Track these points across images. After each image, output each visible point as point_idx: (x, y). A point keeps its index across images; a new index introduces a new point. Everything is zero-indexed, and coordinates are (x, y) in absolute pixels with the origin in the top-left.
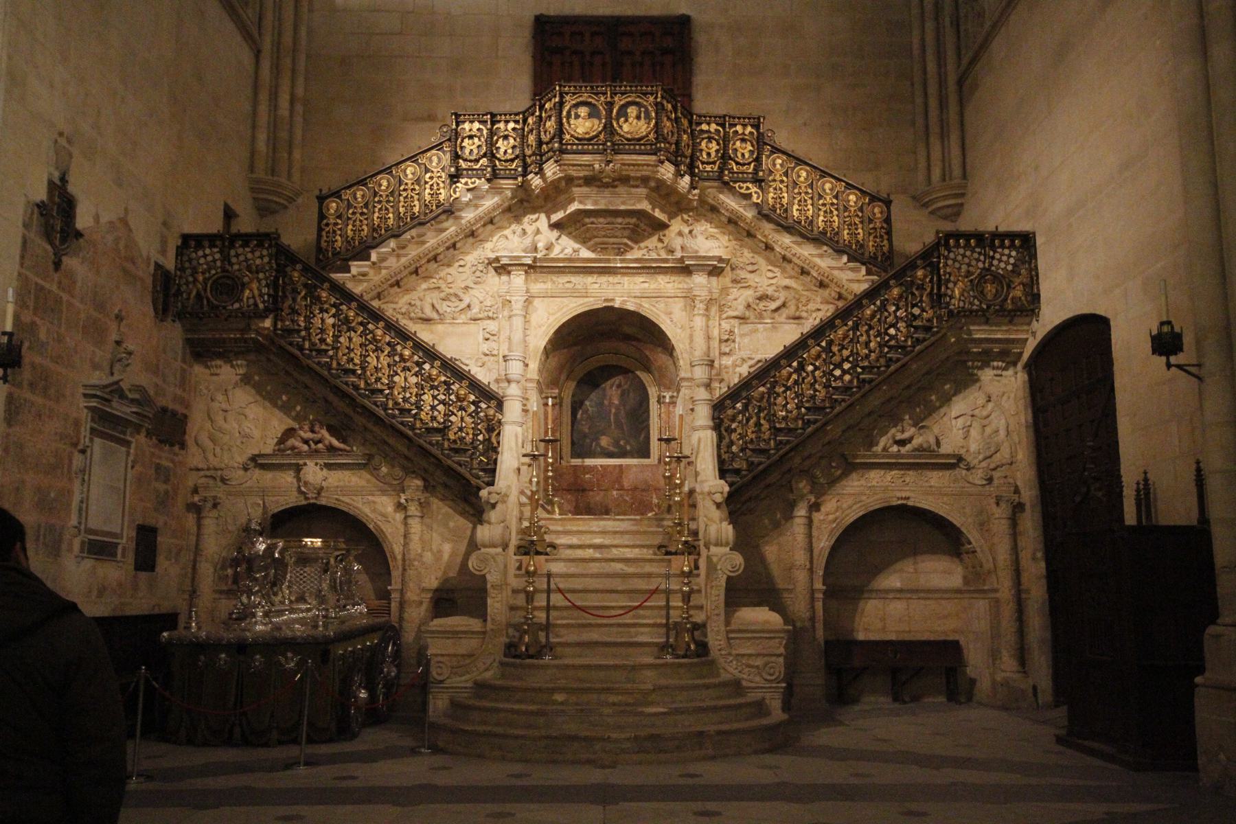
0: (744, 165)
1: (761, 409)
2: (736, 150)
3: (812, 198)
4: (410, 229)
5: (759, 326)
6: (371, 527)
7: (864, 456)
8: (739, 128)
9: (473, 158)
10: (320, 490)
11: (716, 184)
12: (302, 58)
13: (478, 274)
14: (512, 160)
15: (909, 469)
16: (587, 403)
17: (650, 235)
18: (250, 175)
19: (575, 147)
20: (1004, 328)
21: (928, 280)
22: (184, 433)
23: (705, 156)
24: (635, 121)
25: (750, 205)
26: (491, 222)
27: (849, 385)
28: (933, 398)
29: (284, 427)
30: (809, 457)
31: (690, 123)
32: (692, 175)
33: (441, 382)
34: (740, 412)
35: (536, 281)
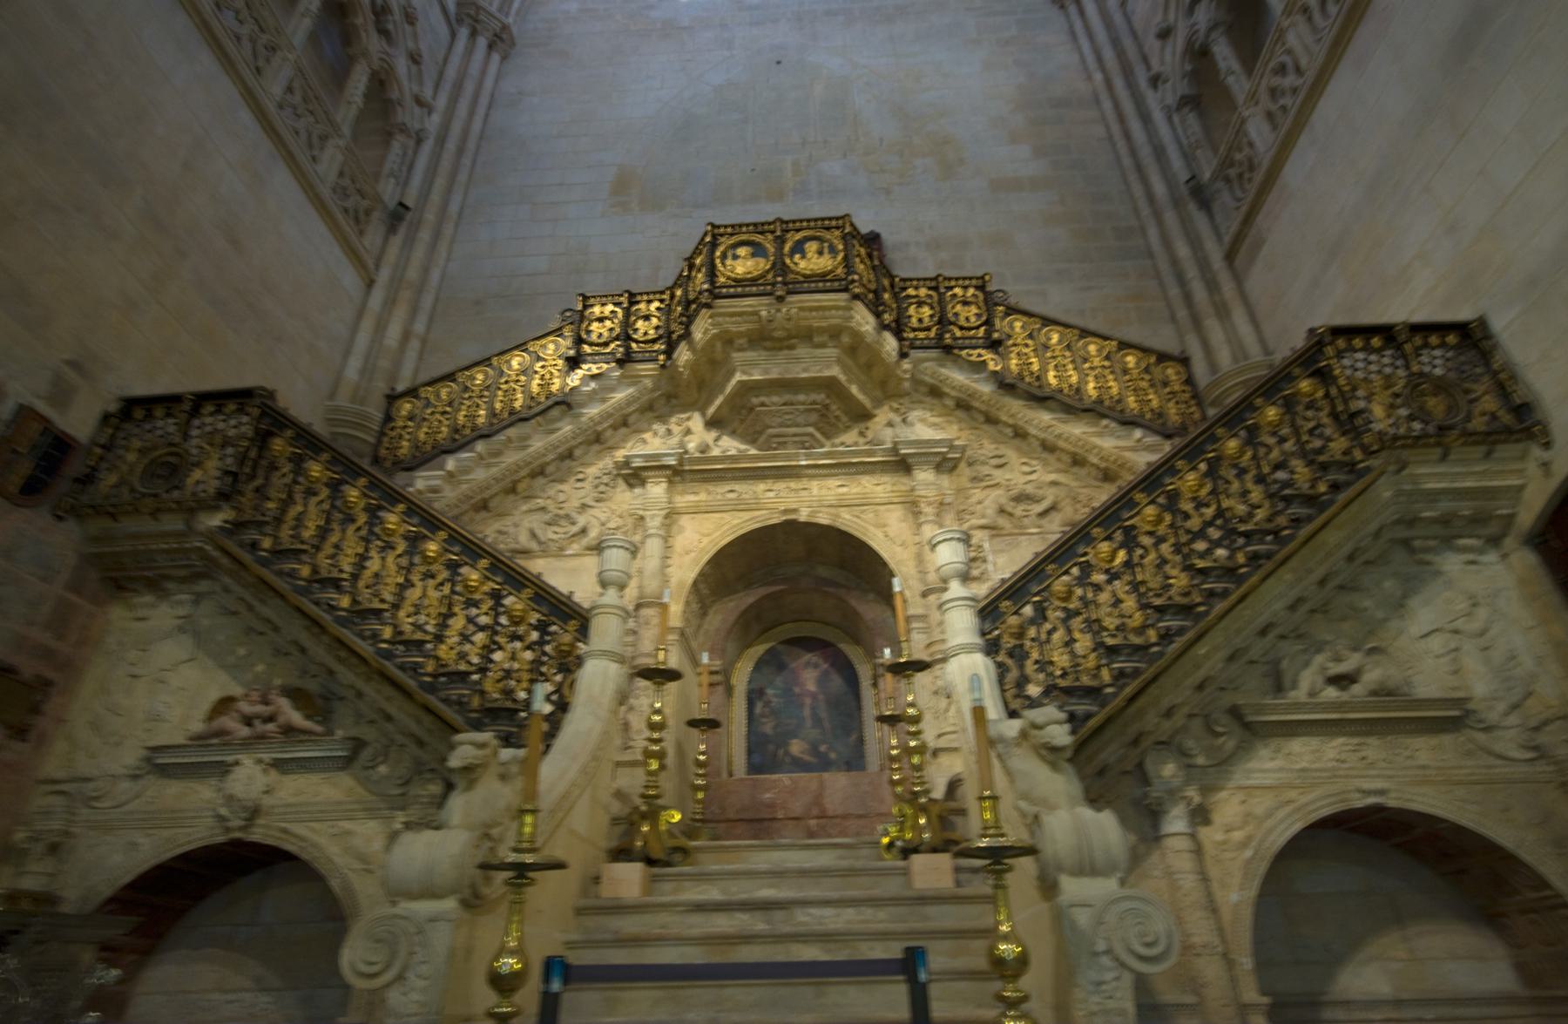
0: (970, 329)
1: (1071, 614)
2: (956, 314)
3: (1073, 362)
4: (505, 428)
5: (1023, 538)
6: (335, 884)
7: (1274, 709)
8: (958, 291)
9: (601, 341)
10: (254, 813)
11: (934, 353)
12: (427, 301)
13: (602, 488)
14: (654, 341)
15: (1368, 734)
16: (770, 692)
17: (848, 428)
18: (329, 403)
19: (732, 290)
20: (1477, 469)
21: (1320, 394)
22: (35, 710)
23: (914, 320)
24: (816, 256)
25: (987, 380)
26: (625, 424)
27: (1230, 564)
28: (1367, 603)
29: (214, 695)
30: (1169, 713)
31: (892, 286)
32: (900, 339)
33: (486, 594)
34: (1032, 621)
35: (684, 493)
